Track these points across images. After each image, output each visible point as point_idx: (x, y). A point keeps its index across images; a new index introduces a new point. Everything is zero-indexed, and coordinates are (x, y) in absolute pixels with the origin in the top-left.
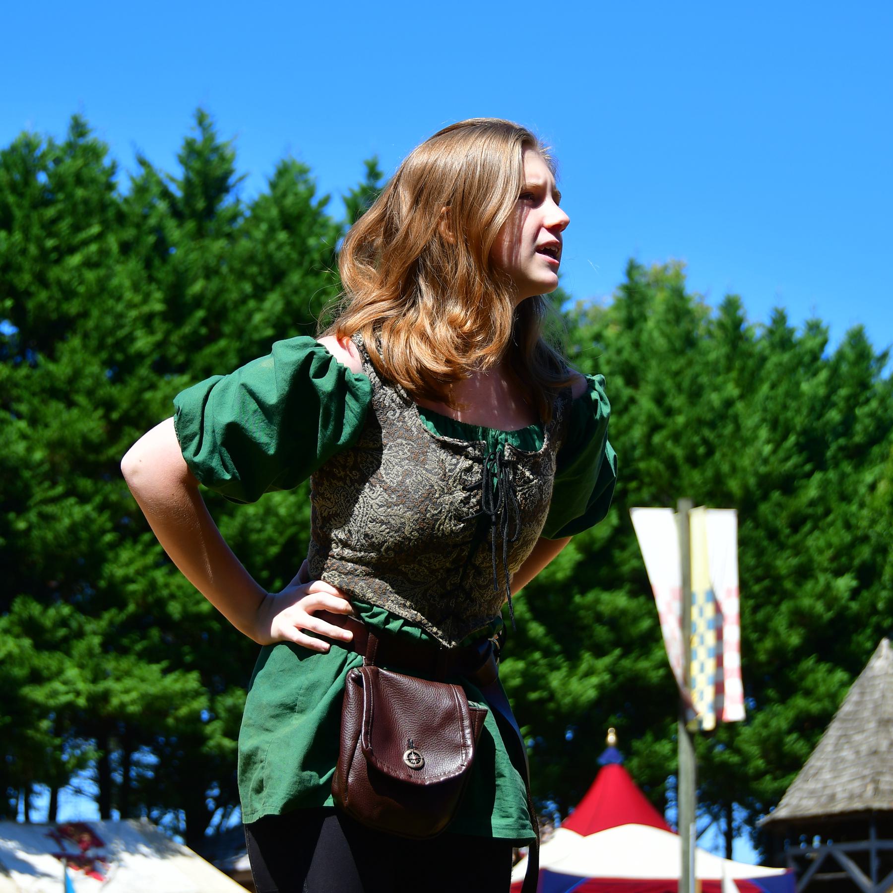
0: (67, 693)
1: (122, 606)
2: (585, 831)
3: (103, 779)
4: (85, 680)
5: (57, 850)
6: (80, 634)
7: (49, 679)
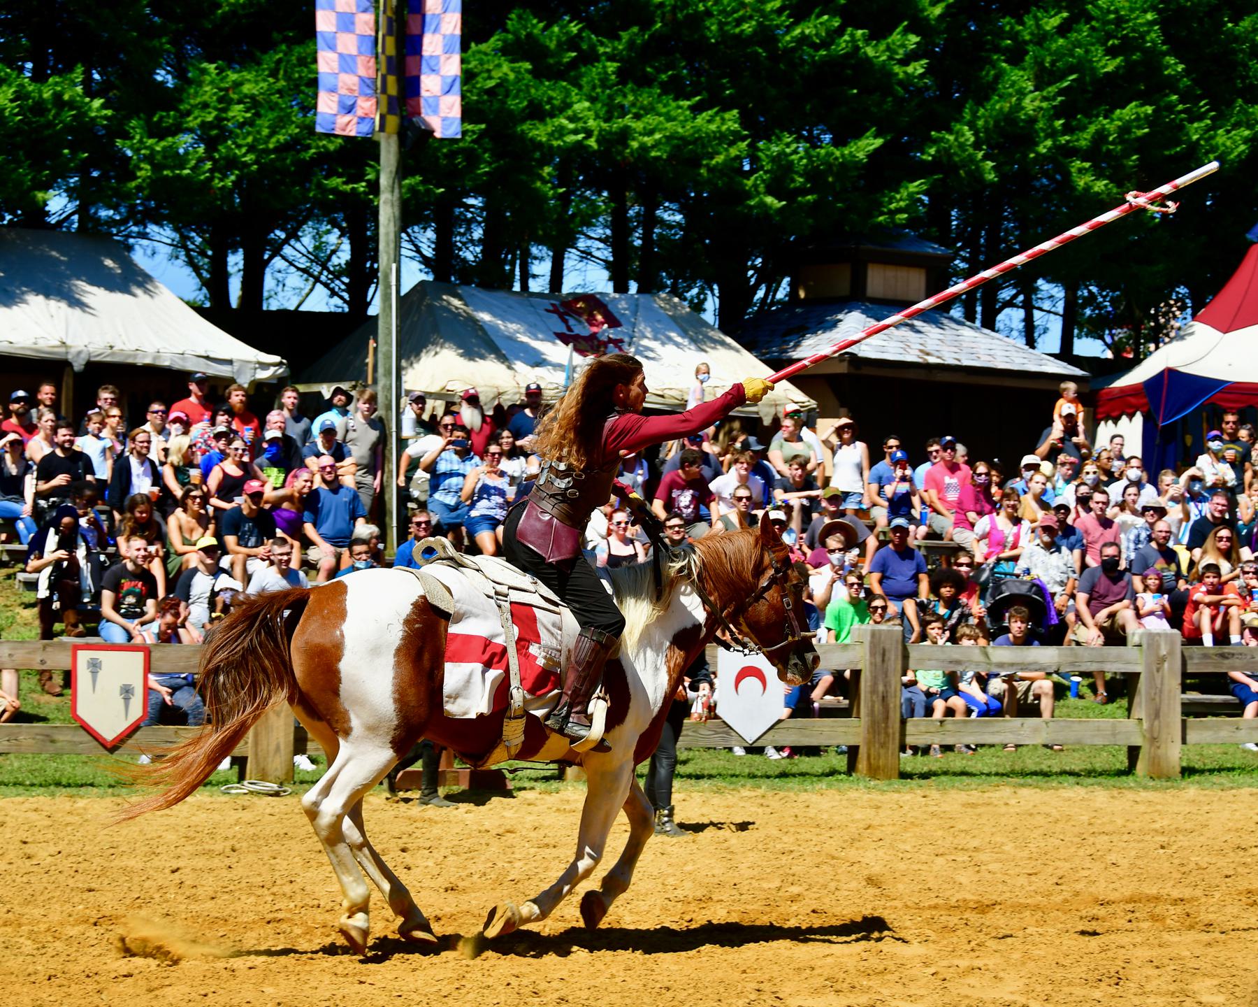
0: (575, 132)
1: (646, 24)
2: (1227, 325)
3: (618, 241)
4: (597, 117)
5: (562, 329)
6: (590, 57)
7: (552, 115)
